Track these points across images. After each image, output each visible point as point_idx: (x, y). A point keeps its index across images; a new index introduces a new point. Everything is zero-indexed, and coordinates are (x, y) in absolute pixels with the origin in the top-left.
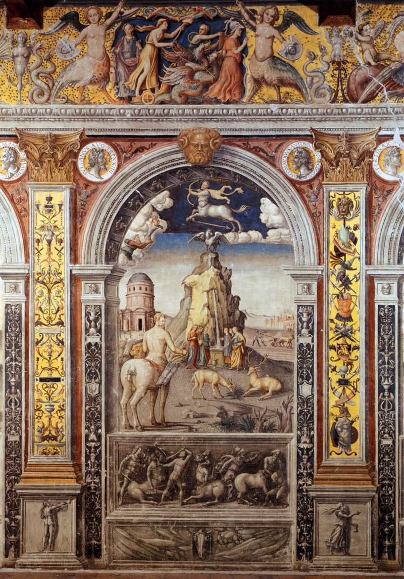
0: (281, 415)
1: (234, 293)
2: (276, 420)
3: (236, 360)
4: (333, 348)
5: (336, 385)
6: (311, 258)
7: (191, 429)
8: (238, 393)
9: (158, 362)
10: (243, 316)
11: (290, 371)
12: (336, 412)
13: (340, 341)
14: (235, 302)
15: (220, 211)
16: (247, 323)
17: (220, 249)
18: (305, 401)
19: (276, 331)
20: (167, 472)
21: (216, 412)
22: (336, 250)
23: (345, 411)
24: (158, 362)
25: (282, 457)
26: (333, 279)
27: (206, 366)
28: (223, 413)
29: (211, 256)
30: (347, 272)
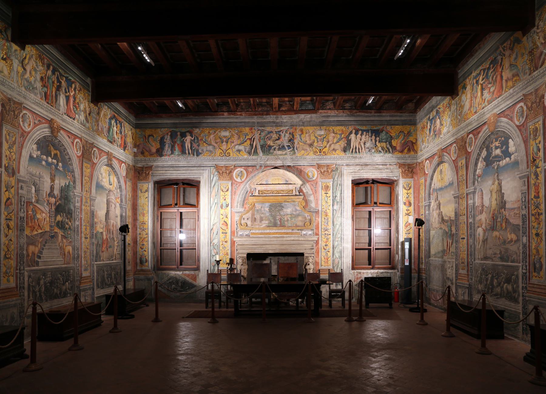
0: (517, 254)
1: (503, 191)
2: (514, 256)
3: (504, 225)
4: (533, 215)
5: (534, 236)
6: (525, 165)
7: (493, 261)
8: (504, 242)
9: (485, 229)
10: (505, 203)
11: (519, 230)
12: (534, 252)
13: (535, 211)
14: (502, 195)
15: (498, 152)
16: (507, 207)
17: (499, 170)
18: (524, 246)
19: (514, 209)
20: (487, 280)
21: (498, 252)
22: (533, 158)
23: (538, 251)
24: (485, 229)
25: (517, 276)
26: (532, 175)
27: (496, 230)
28: (501, 252)
29: (496, 175)
30: (537, 169)
